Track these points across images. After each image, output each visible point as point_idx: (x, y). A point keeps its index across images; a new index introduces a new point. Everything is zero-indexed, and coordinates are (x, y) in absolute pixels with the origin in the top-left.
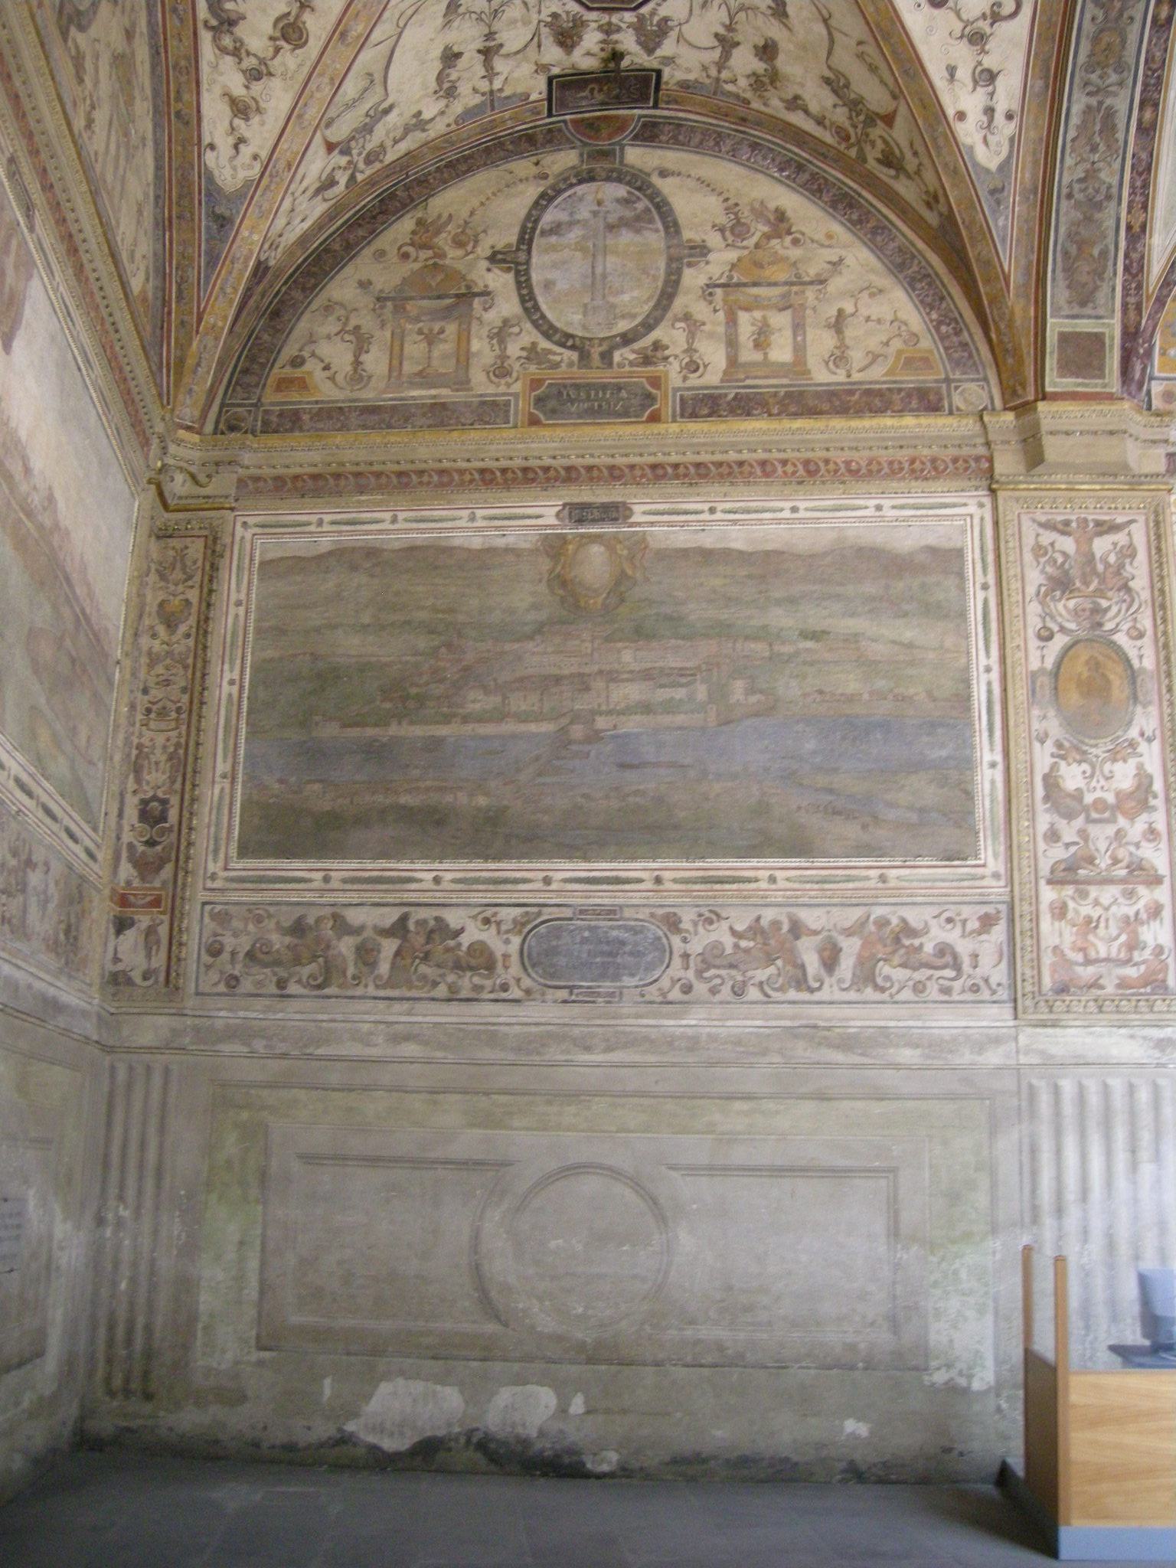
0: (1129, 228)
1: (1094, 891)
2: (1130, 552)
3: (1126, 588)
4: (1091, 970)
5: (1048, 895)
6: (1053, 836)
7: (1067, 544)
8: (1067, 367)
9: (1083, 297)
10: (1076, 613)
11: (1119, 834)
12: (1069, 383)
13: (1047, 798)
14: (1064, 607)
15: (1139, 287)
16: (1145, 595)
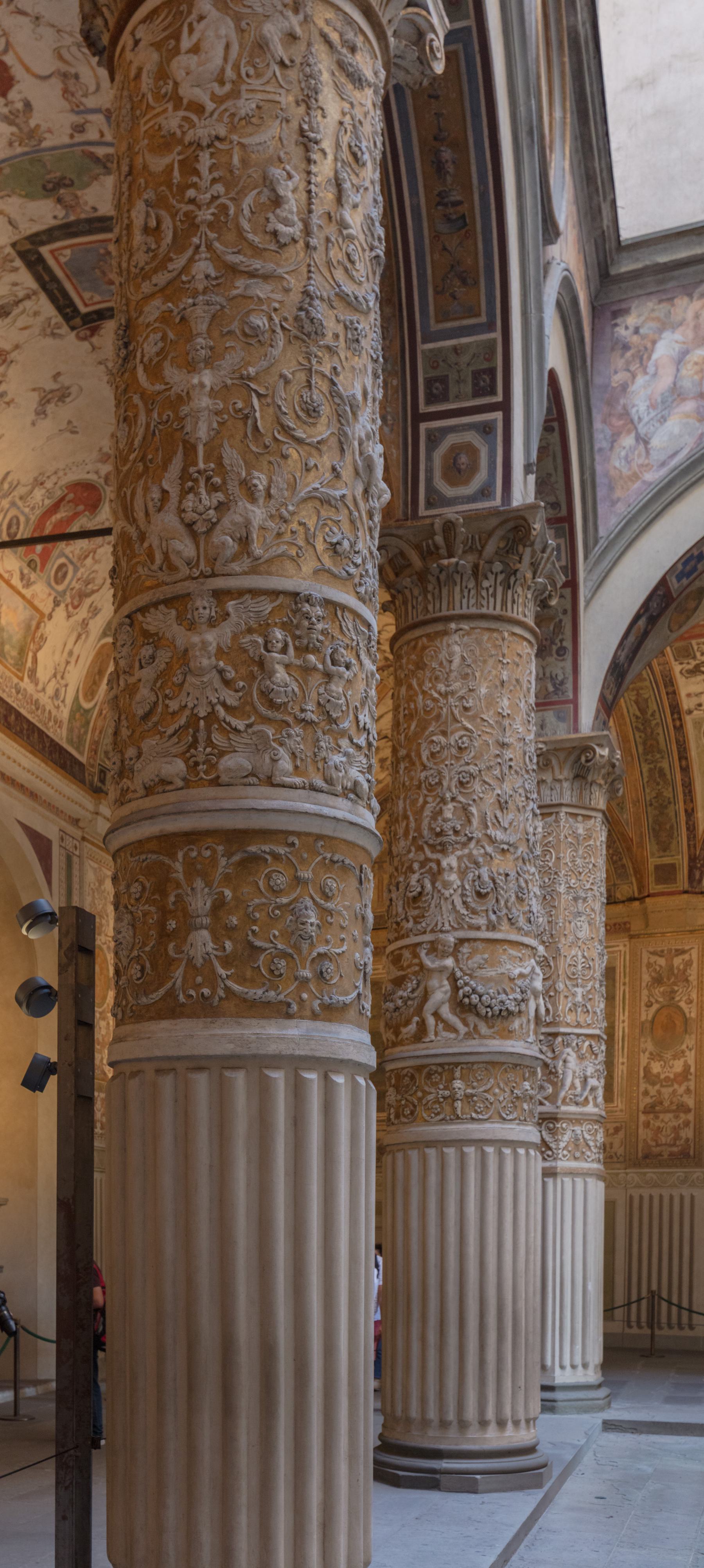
0: (686, 811)
1: (661, 1116)
2: (689, 964)
3: (687, 980)
4: (658, 1149)
5: (642, 1118)
6: (646, 1093)
7: (662, 962)
8: (659, 881)
9: (664, 847)
10: (663, 994)
11: (674, 1091)
12: (660, 888)
13: (645, 1077)
14: (658, 991)
15: (694, 837)
16: (695, 983)
